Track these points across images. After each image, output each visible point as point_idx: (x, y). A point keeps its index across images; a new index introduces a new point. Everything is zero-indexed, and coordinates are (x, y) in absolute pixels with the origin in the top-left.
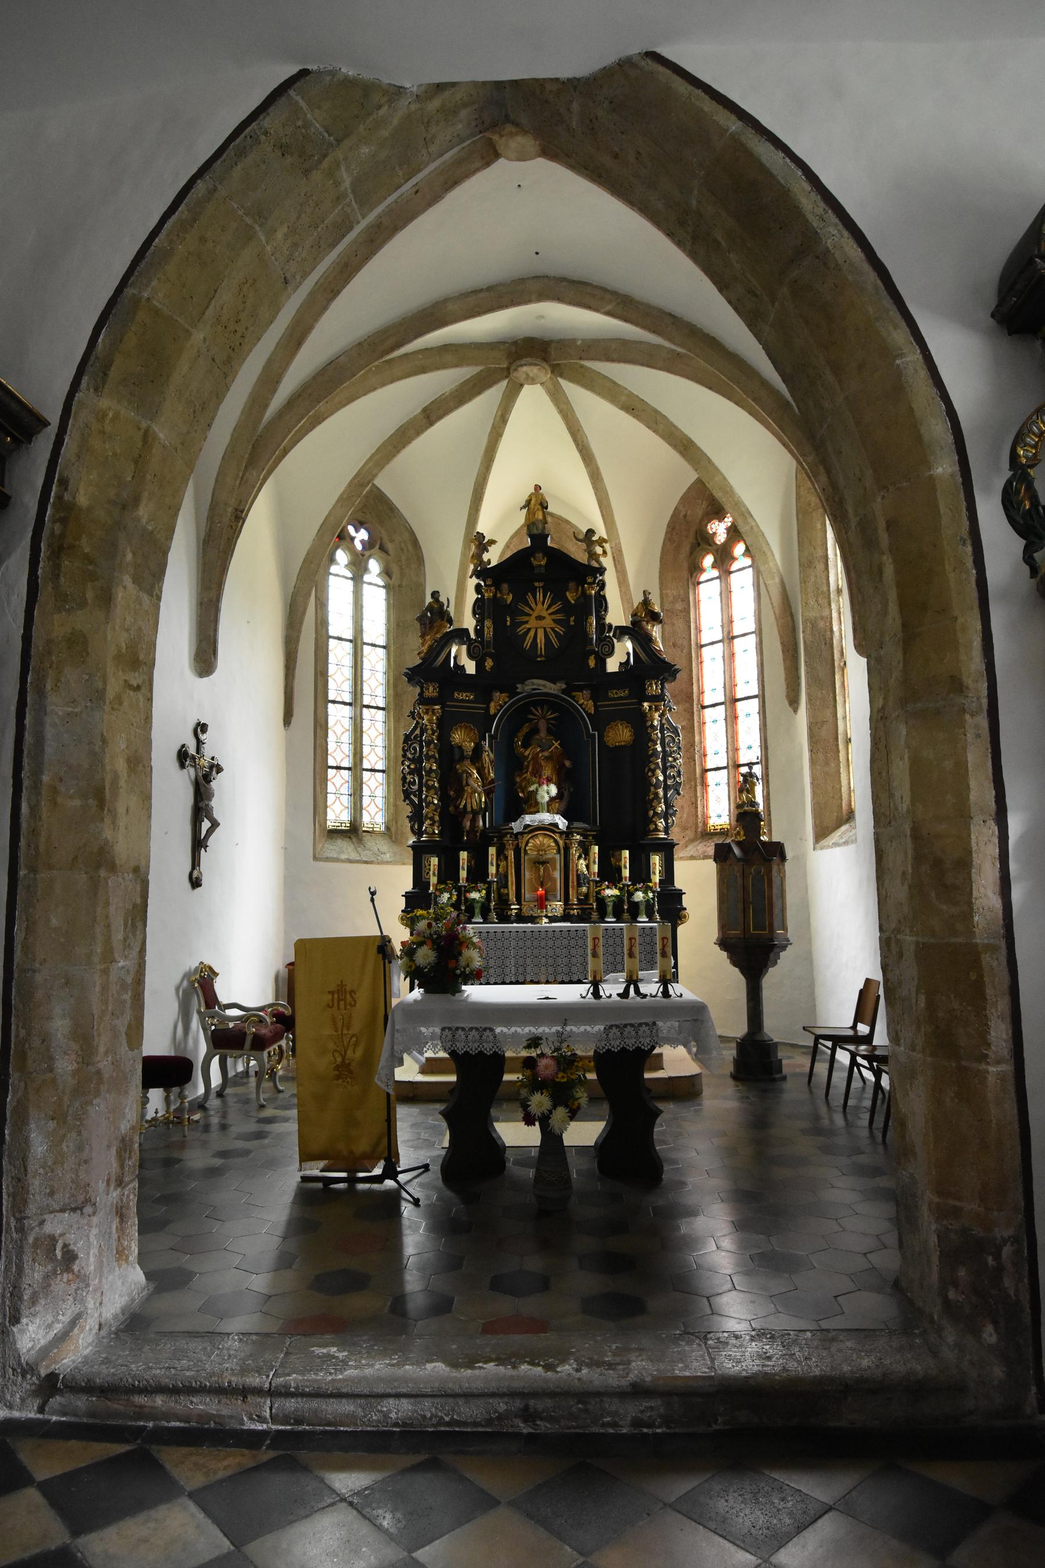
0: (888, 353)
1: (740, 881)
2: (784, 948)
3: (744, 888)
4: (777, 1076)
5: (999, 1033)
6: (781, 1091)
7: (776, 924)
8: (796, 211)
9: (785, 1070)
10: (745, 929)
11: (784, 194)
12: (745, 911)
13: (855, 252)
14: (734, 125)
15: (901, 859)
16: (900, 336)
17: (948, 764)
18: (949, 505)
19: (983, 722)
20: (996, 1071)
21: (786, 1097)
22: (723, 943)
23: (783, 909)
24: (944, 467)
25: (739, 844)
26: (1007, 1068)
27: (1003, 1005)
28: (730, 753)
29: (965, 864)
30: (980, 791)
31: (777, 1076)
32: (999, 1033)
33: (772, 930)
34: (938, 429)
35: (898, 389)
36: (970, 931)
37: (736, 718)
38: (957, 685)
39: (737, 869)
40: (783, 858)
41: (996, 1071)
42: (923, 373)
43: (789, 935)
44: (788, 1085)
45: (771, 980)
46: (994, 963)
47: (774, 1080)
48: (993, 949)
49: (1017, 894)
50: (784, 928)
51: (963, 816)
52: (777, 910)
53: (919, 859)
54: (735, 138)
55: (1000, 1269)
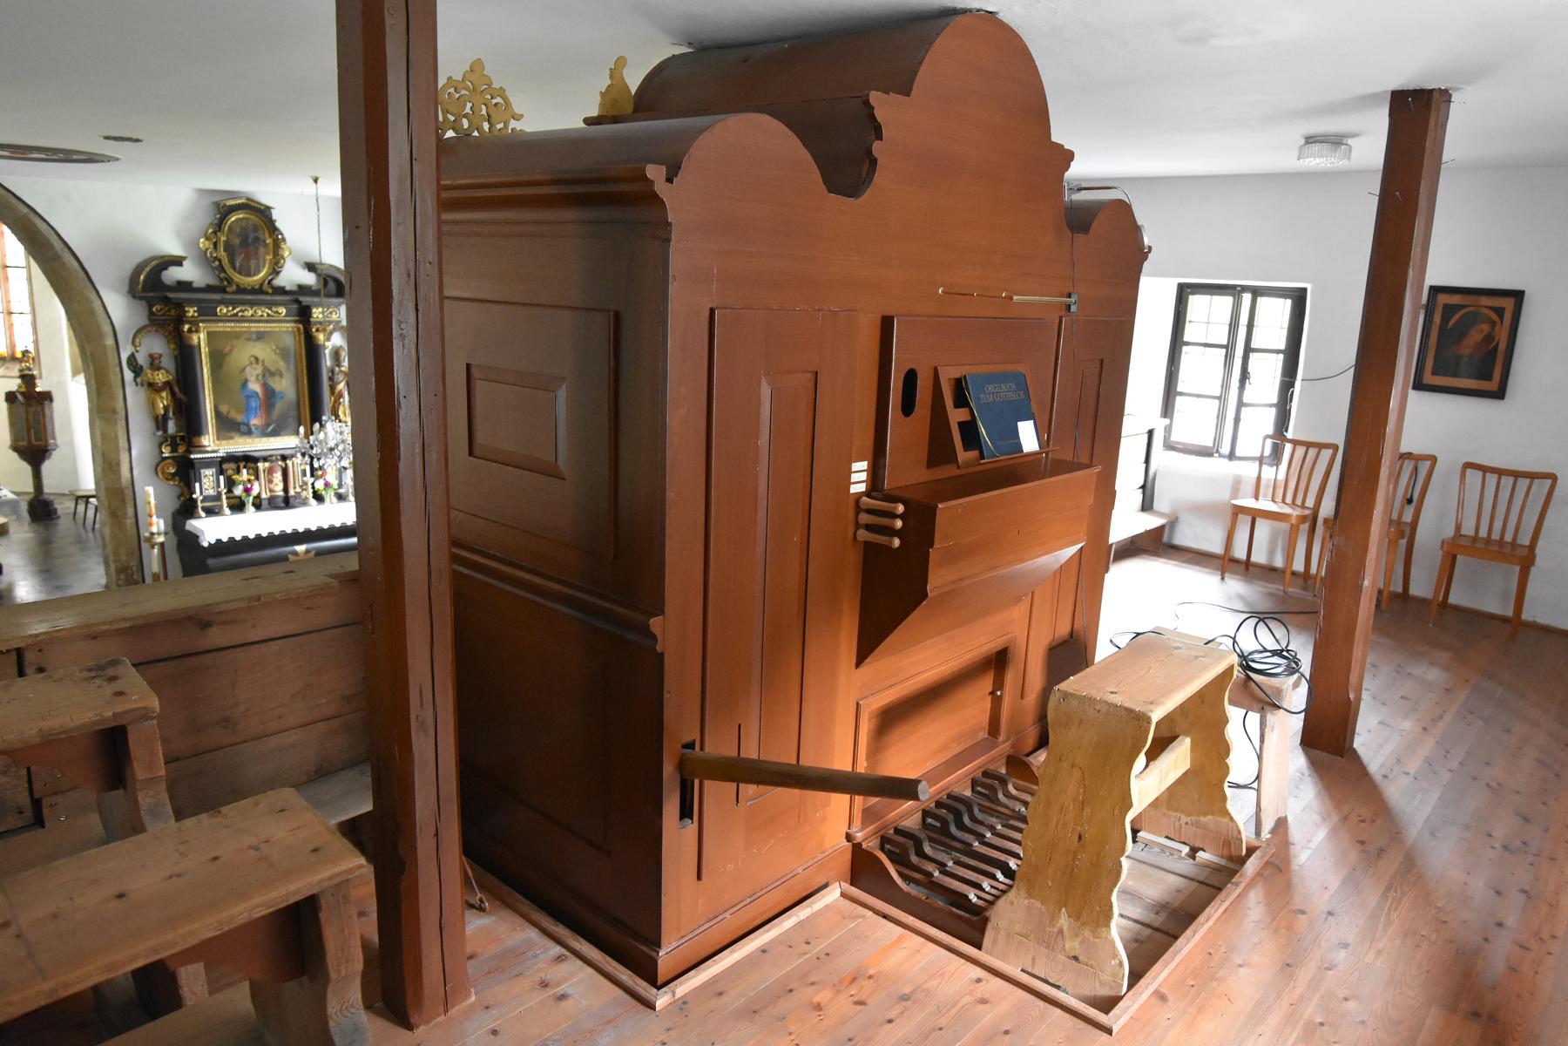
0: (88, 301)
1: (24, 416)
2: (54, 450)
3: (27, 419)
4: (54, 516)
5: (130, 511)
6: (57, 525)
7: (49, 437)
8: (52, 246)
9: (59, 513)
10: (30, 440)
11: (47, 239)
12: (28, 432)
13: (76, 264)
14: (26, 210)
15: (99, 459)
16: (93, 296)
17: (113, 435)
18: (112, 355)
19: (124, 422)
20: (130, 521)
21: (60, 527)
22: (15, 448)
23: (53, 428)
24: (110, 342)
25: (22, 393)
26: (133, 520)
27: (132, 503)
28: (4, 304)
29: (118, 464)
30: (123, 443)
31: (54, 516)
32: (130, 511)
33: (46, 441)
34: (107, 329)
35: (92, 313)
36: (120, 483)
37: (7, 279)
38: (114, 411)
39: (22, 409)
40: (51, 400)
41: (130, 521)
42: (102, 309)
43: (58, 443)
44: (60, 521)
45: (46, 467)
46: (128, 492)
47: (52, 519)
48: (127, 488)
49: (135, 472)
50: (54, 438)
51: (117, 450)
52: (49, 430)
53: (104, 461)
54: (25, 216)
55: (133, 573)
